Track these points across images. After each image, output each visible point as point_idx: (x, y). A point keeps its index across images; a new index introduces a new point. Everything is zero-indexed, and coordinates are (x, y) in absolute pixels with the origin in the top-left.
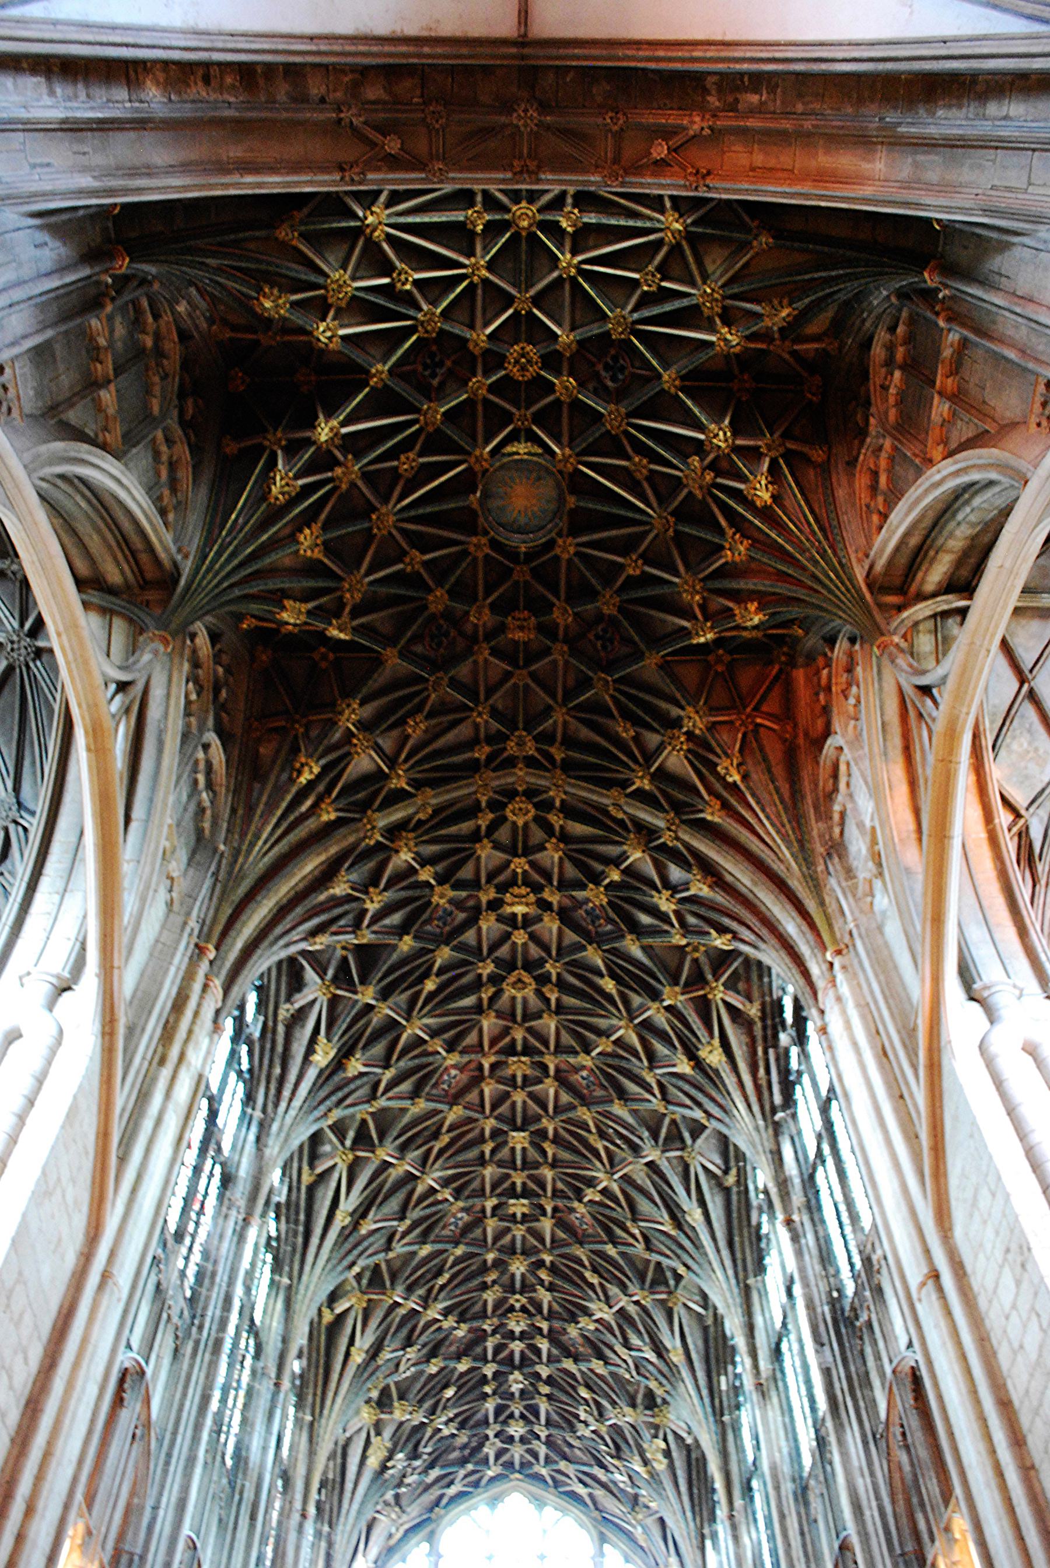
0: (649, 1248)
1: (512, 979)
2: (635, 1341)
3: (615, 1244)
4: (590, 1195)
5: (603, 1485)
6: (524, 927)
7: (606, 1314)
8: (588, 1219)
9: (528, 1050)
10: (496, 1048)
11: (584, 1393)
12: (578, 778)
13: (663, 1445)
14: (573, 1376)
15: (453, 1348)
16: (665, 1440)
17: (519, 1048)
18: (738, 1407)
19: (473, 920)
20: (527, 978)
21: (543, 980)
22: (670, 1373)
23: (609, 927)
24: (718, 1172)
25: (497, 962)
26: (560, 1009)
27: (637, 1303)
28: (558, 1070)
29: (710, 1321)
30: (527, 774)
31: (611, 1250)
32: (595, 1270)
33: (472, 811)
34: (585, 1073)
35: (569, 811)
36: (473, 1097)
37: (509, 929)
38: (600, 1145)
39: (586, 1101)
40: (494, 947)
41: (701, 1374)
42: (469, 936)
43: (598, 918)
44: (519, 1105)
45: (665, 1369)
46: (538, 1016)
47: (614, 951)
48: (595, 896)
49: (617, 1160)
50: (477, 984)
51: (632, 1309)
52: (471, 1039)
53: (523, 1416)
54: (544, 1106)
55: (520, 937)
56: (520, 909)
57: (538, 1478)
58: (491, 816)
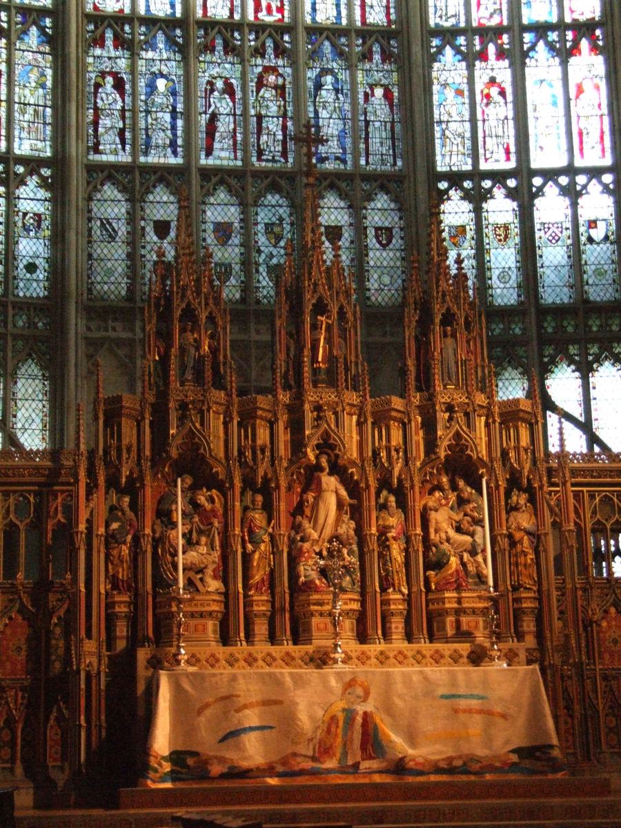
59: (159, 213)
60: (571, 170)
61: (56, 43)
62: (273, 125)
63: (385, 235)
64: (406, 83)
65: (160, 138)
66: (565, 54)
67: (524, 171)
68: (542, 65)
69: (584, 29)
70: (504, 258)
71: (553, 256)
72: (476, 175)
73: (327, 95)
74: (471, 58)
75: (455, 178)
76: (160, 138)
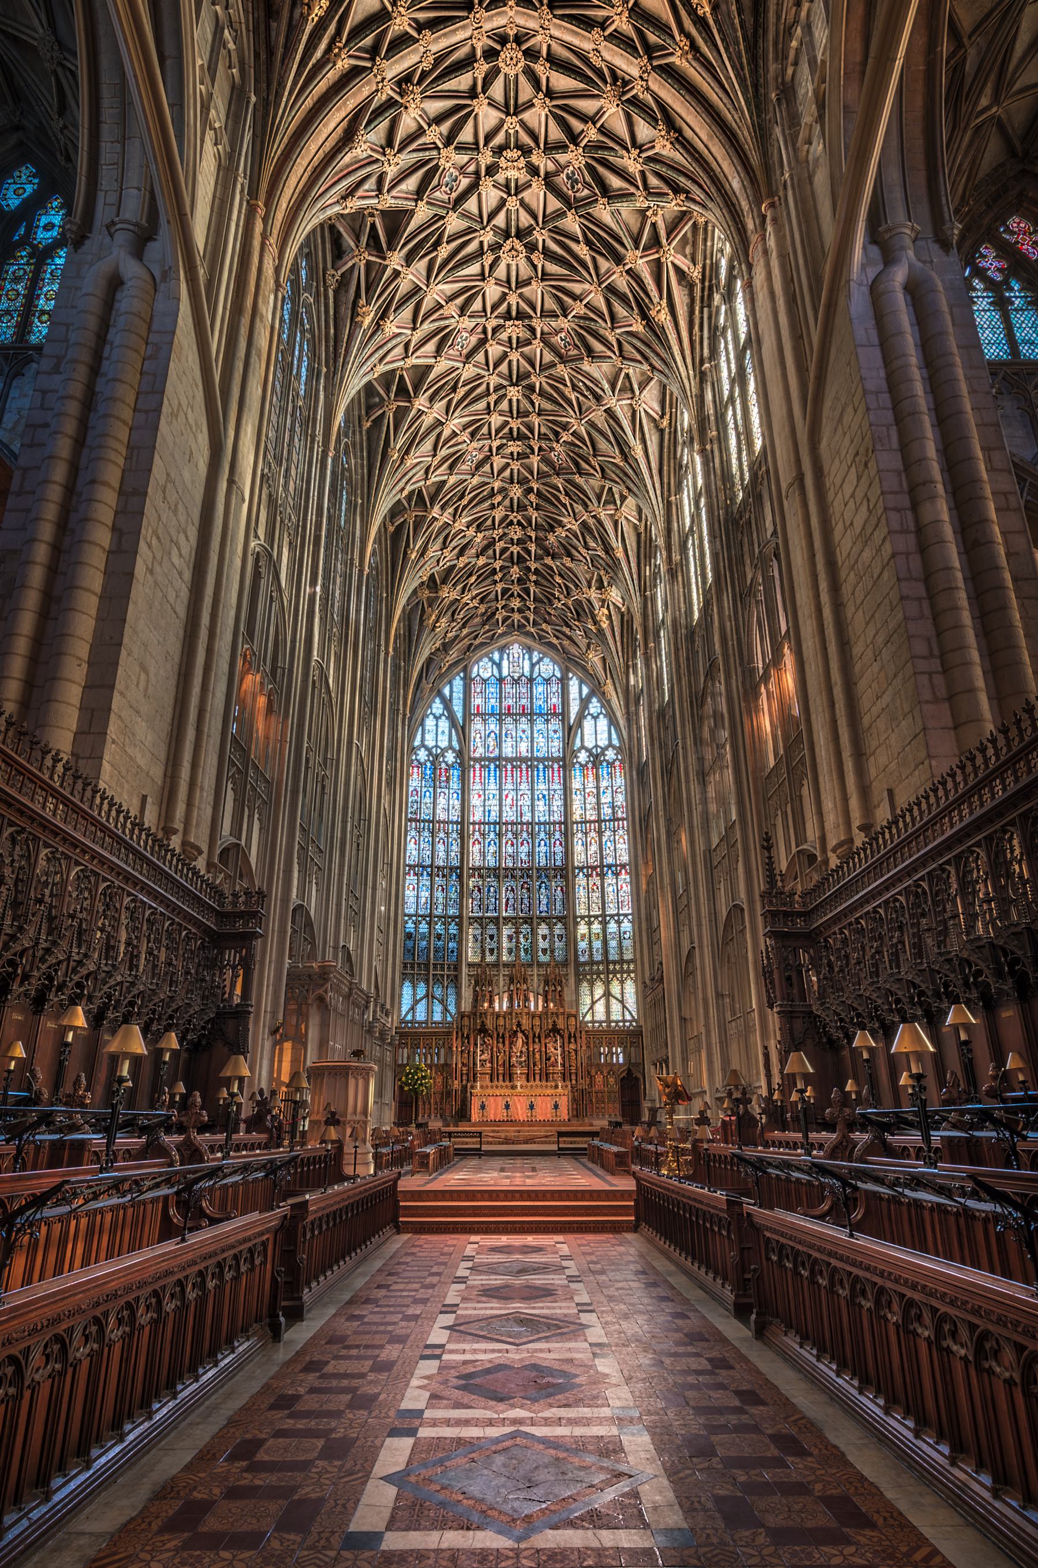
0: (603, 477)
1: (507, 247)
2: (592, 544)
3: (581, 474)
4: (565, 437)
5: (570, 638)
6: (516, 195)
7: (575, 527)
8: (563, 456)
9: (521, 316)
10: (496, 314)
11: (558, 579)
12: (562, 17)
13: (606, 612)
14: (551, 569)
15: (474, 551)
16: (608, 608)
17: (514, 313)
18: (655, 586)
19: (474, 187)
20: (518, 245)
21: (531, 248)
22: (613, 566)
23: (586, 192)
24: (657, 417)
25: (496, 229)
26: (545, 276)
27: (594, 517)
28: (542, 333)
29: (642, 530)
30: (517, 12)
31: (579, 480)
32: (567, 494)
33: (467, 63)
34: (563, 335)
35: (553, 61)
36: (480, 357)
37: (505, 196)
38: (573, 396)
39: (564, 360)
40: (492, 215)
41: (633, 565)
42: (471, 205)
43: (576, 181)
44: (515, 363)
45: (610, 562)
46: (527, 283)
47: (589, 217)
48: (574, 158)
49: (584, 409)
50: (480, 253)
51: (591, 522)
52: (477, 305)
53: (519, 595)
54: (533, 366)
55: (512, 203)
56: (512, 174)
57: (529, 634)
58: (486, 67)
59: (491, 932)
60: (618, 915)
61: (460, 877)
62: (526, 901)
63: (560, 937)
64: (567, 886)
65: (491, 907)
66: (617, 875)
67: (604, 915)
68: (610, 879)
69: (623, 866)
70: (597, 944)
71: (613, 944)
72: (589, 916)
73: (543, 890)
74: (588, 876)
75: (582, 917)
76: (491, 907)
